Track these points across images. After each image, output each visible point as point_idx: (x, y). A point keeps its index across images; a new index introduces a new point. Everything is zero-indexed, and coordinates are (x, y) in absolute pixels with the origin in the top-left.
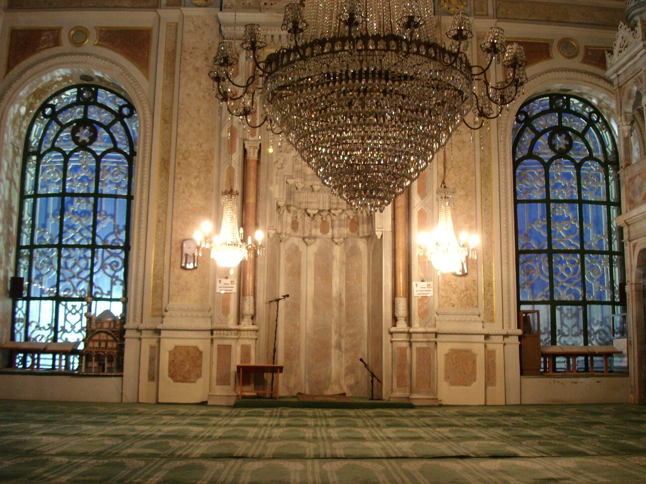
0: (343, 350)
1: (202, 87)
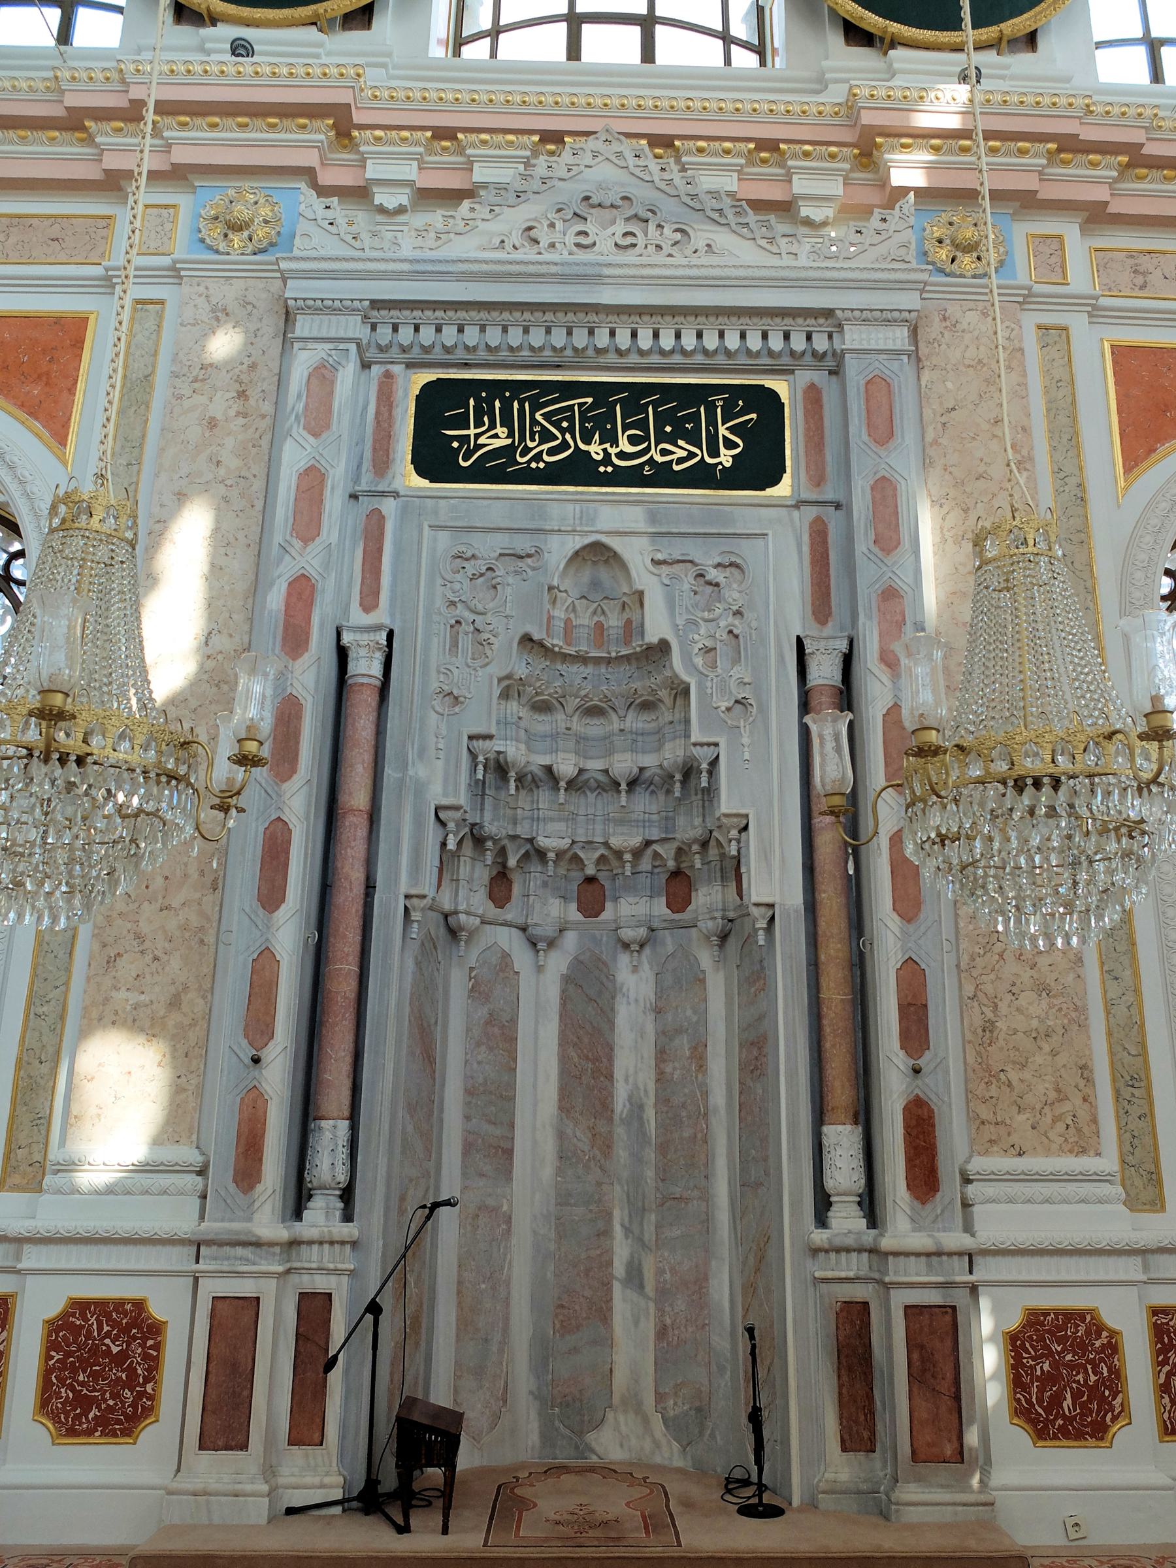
1: (222, 472)
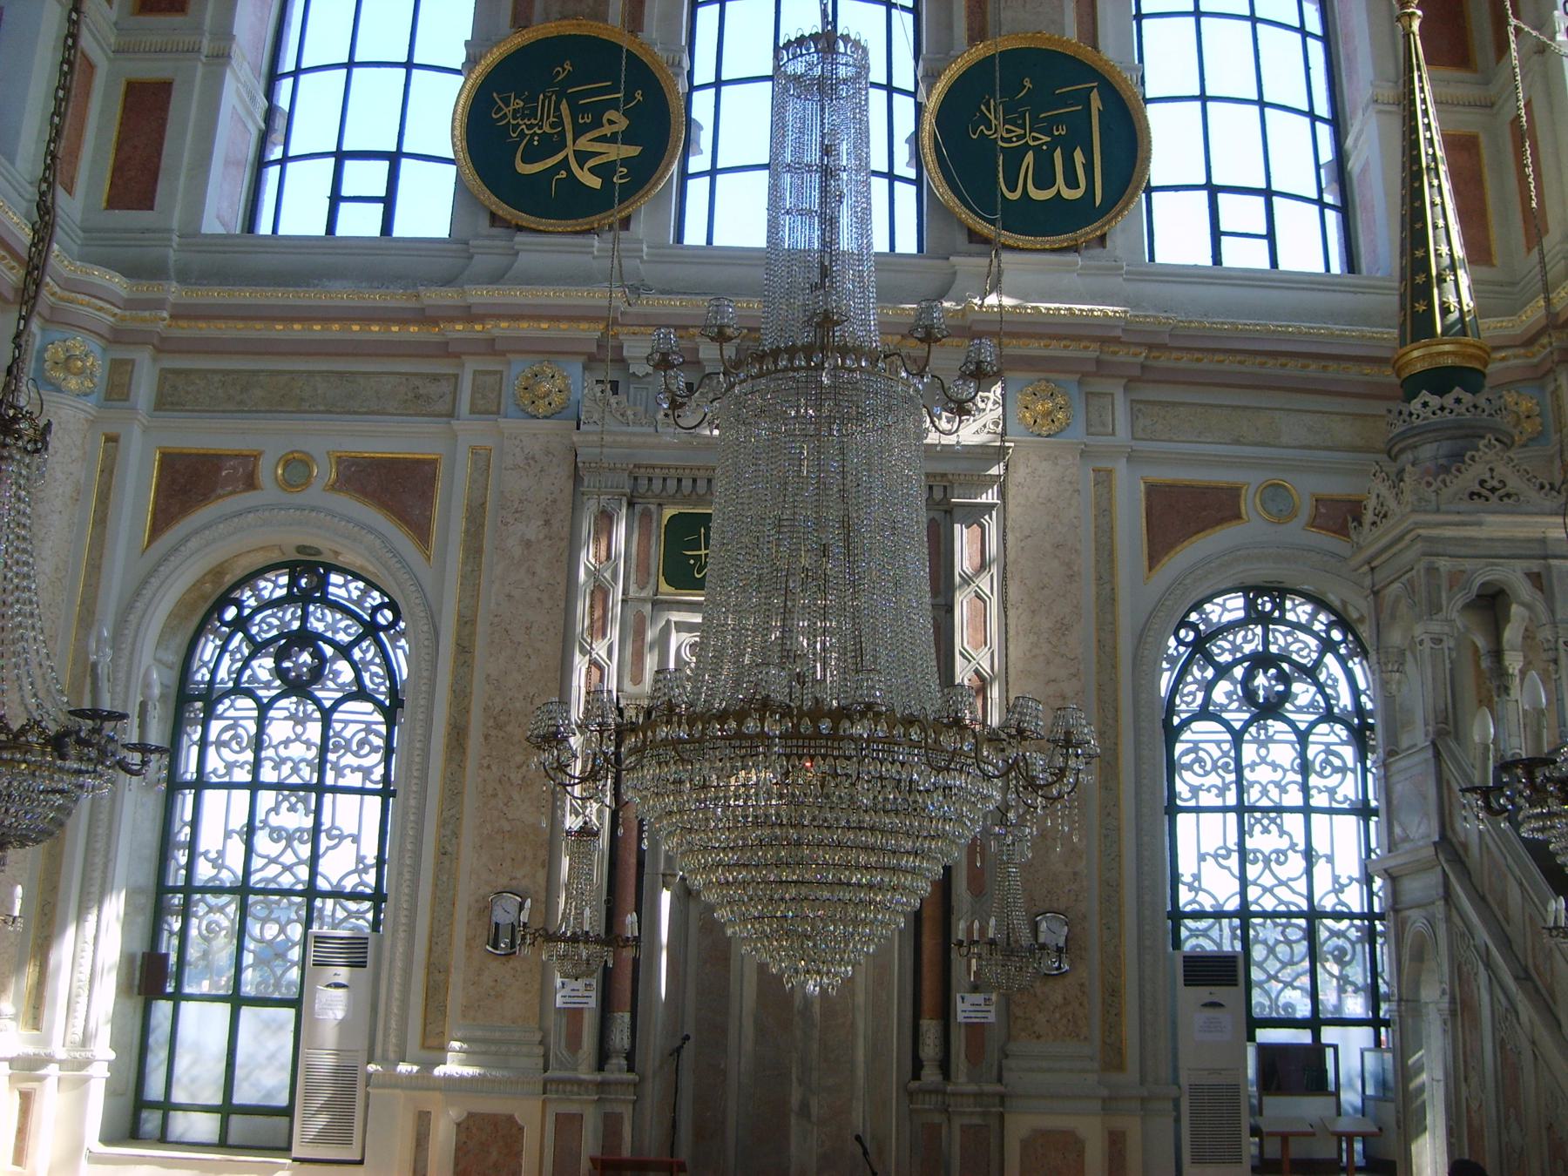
0: (814, 1119)
